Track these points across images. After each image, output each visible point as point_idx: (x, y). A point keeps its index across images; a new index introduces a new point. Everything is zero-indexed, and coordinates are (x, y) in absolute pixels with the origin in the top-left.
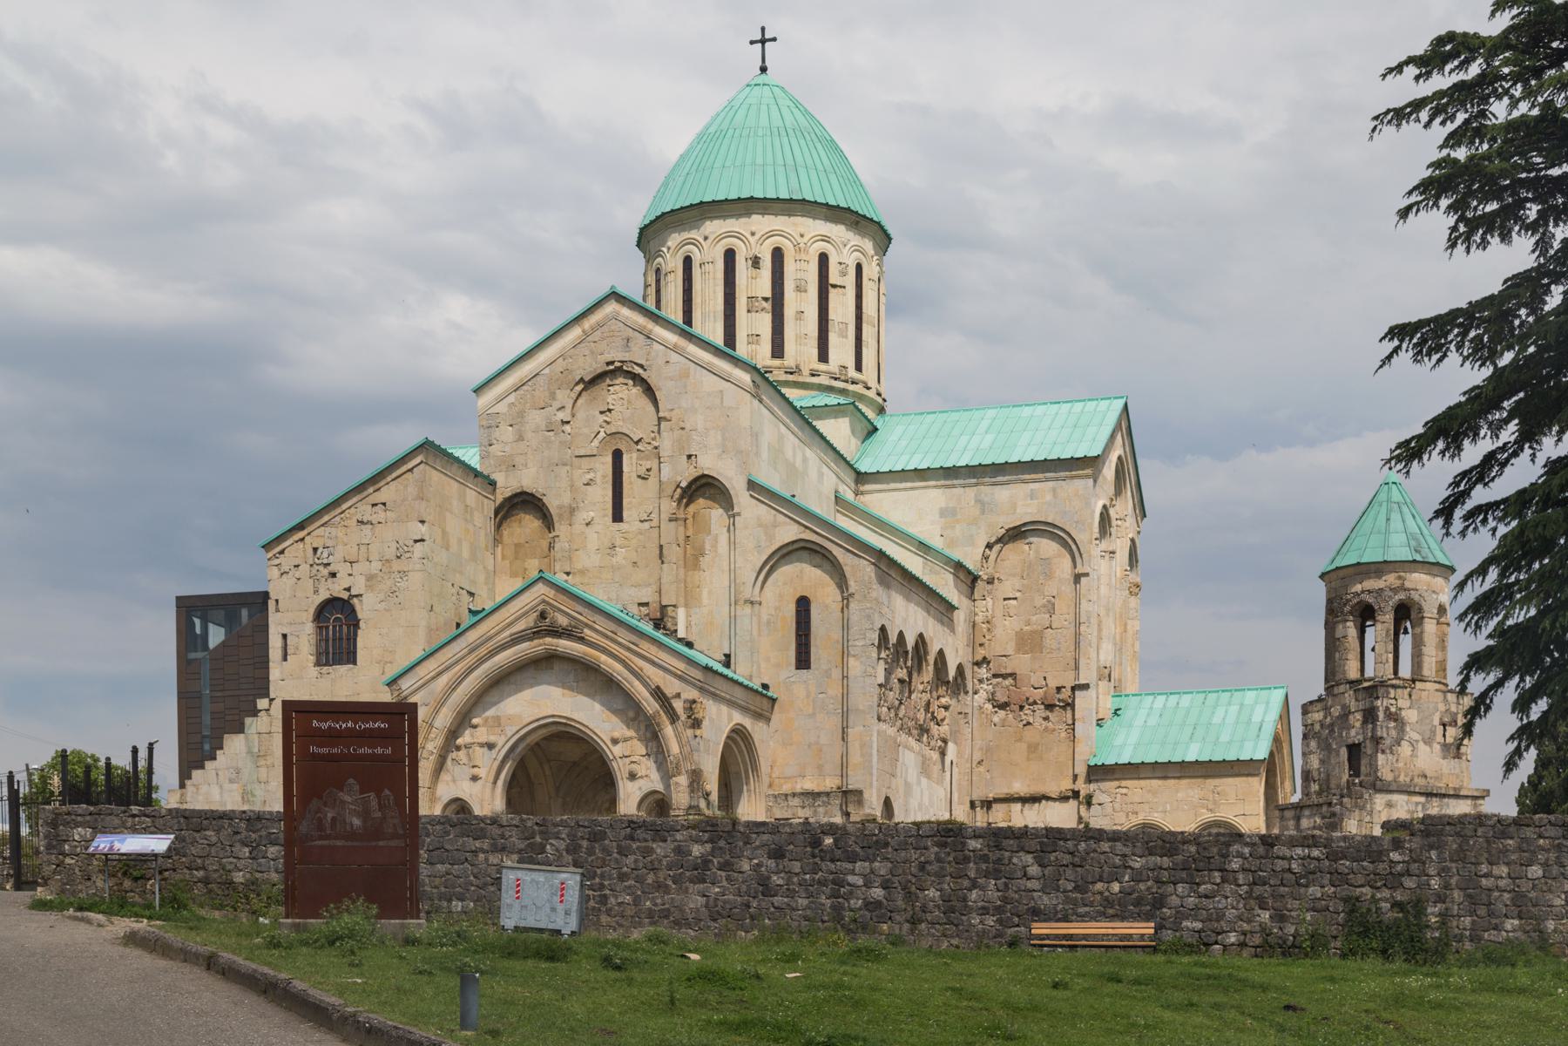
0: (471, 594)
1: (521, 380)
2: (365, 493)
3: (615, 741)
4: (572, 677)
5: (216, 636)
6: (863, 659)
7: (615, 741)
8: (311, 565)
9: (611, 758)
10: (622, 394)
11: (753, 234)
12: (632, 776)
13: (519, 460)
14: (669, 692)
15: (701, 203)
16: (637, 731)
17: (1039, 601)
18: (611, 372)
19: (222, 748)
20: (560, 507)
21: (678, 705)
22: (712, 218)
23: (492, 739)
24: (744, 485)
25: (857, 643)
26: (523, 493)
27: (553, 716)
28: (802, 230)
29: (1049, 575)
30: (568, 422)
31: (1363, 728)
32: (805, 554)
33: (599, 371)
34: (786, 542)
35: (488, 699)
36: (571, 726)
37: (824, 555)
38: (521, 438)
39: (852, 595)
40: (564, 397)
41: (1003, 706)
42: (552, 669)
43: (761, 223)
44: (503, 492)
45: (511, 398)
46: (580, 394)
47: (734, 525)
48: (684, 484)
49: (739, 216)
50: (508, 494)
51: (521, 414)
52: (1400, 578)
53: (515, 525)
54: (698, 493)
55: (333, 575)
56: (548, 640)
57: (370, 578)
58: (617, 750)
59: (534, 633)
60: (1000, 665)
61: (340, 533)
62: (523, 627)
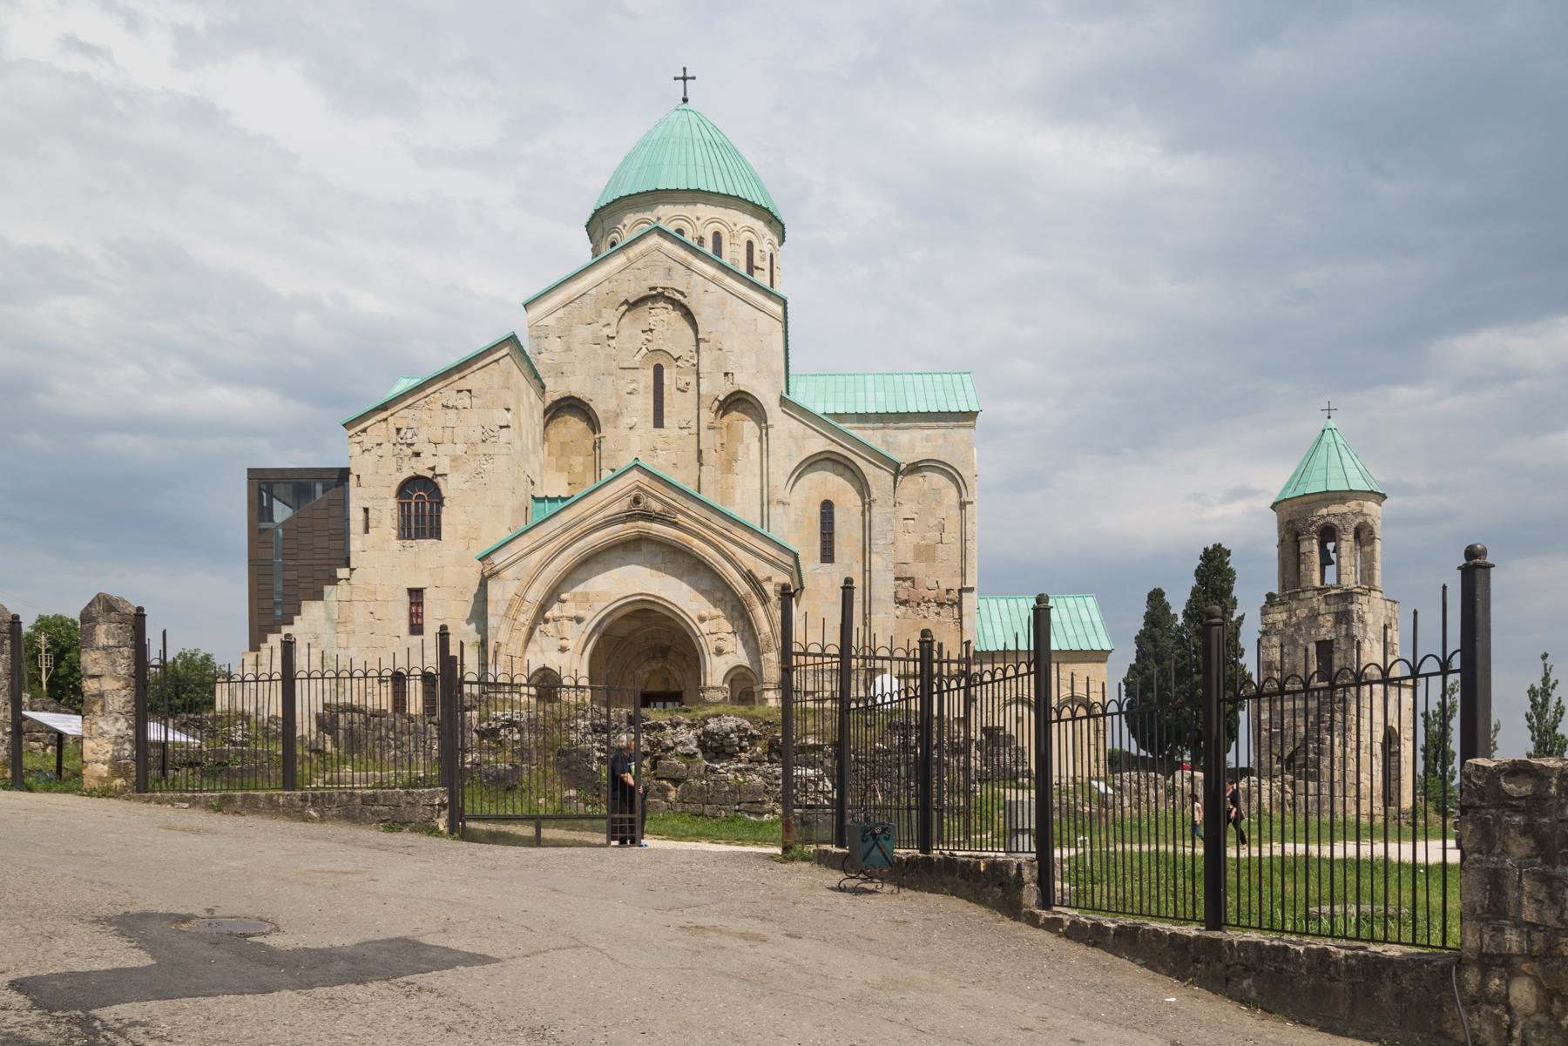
0: (533, 483)
1: (570, 298)
2: (450, 380)
3: (702, 619)
4: (659, 559)
5: (281, 513)
6: (885, 556)
7: (702, 619)
8: (394, 445)
9: (698, 634)
10: (663, 318)
11: (698, 219)
12: (719, 652)
13: (566, 368)
14: (760, 575)
15: (657, 190)
16: (724, 610)
17: (933, 522)
18: (654, 297)
19: (299, 613)
20: (606, 412)
21: (769, 588)
22: (664, 203)
23: (581, 613)
24: (777, 402)
25: (878, 542)
26: (571, 398)
27: (641, 594)
28: (735, 220)
29: (939, 502)
30: (613, 338)
31: (1335, 627)
32: (829, 464)
33: (642, 295)
34: (815, 452)
35: (577, 576)
36: (658, 604)
37: (845, 465)
38: (569, 349)
39: (874, 500)
40: (610, 315)
41: (904, 603)
42: (640, 550)
43: (704, 211)
44: (553, 395)
45: (560, 313)
46: (624, 314)
47: (767, 435)
48: (721, 398)
49: (686, 203)
50: (556, 397)
51: (569, 328)
52: (1359, 504)
53: (561, 425)
54: (732, 407)
55: (417, 455)
56: (641, 523)
57: (455, 459)
58: (704, 627)
59: (627, 516)
60: (901, 571)
61: (425, 415)
62: (617, 510)
